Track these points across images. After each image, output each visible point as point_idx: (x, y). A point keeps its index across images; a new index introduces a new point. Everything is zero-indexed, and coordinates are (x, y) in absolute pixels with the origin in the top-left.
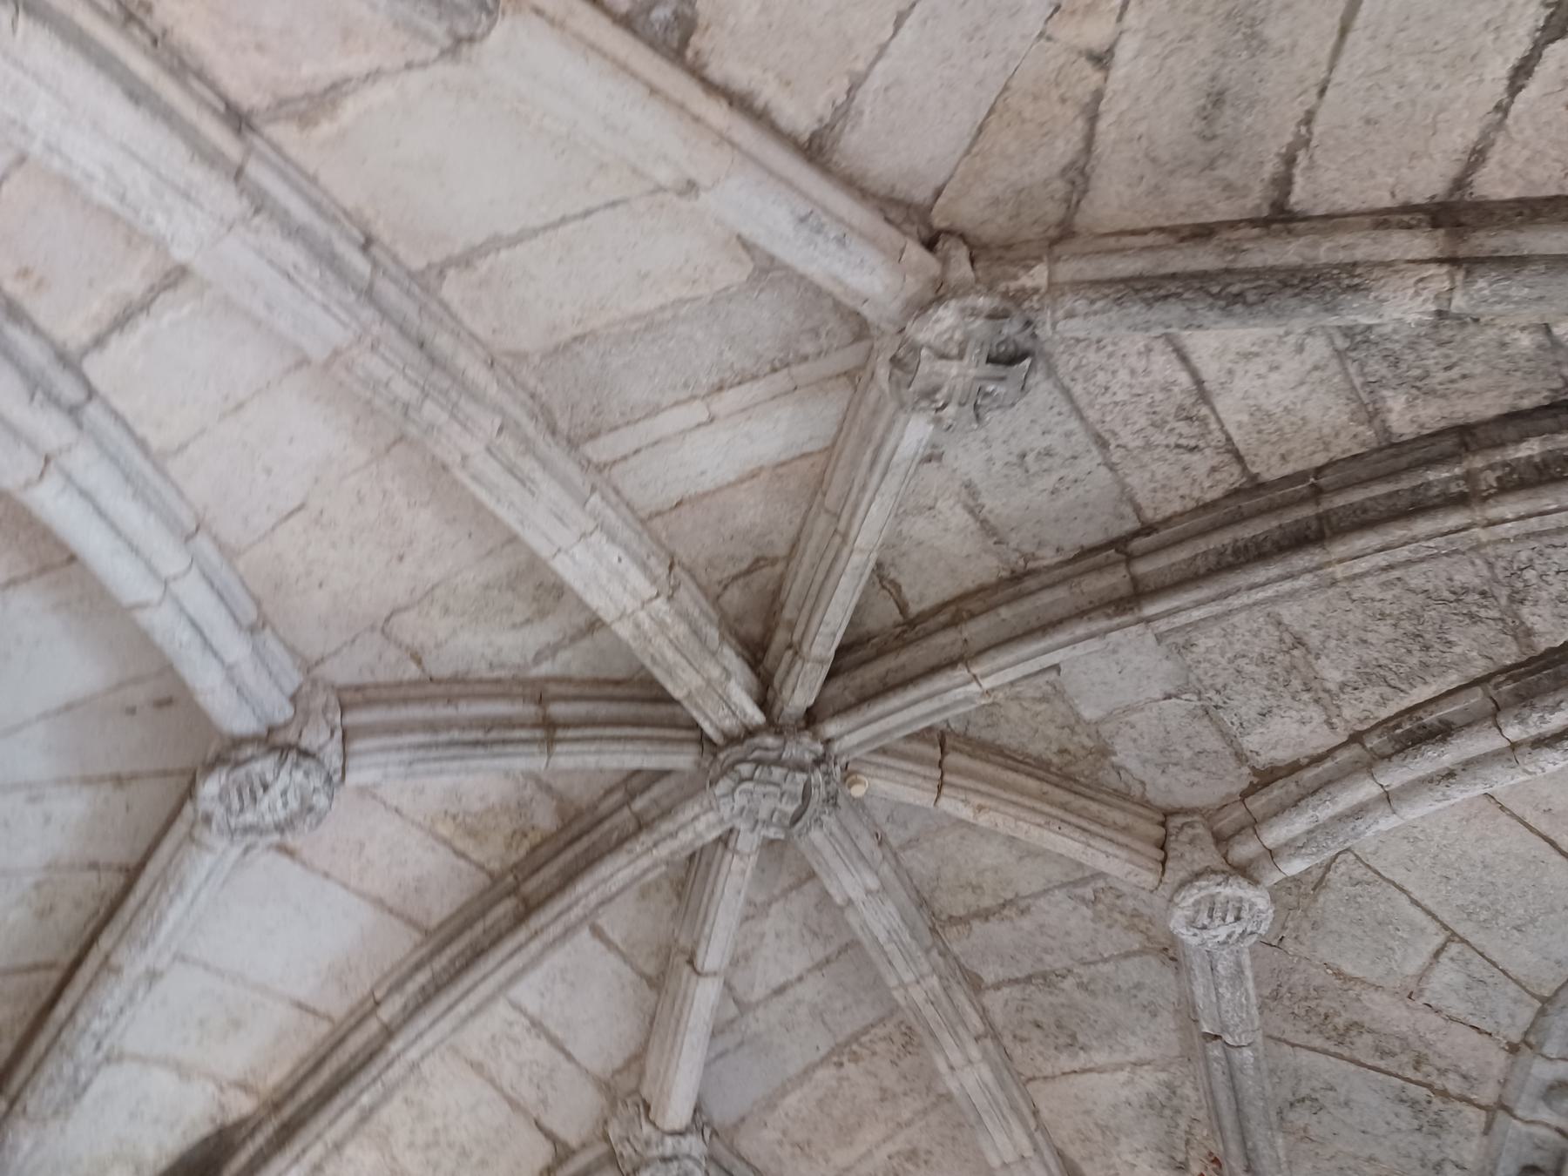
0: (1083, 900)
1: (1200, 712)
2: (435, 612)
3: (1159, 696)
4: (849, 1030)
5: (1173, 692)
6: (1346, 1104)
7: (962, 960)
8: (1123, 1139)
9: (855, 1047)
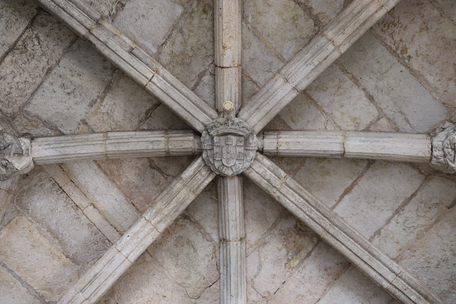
2: (189, 282)
4: (389, 57)
9: (399, 52)
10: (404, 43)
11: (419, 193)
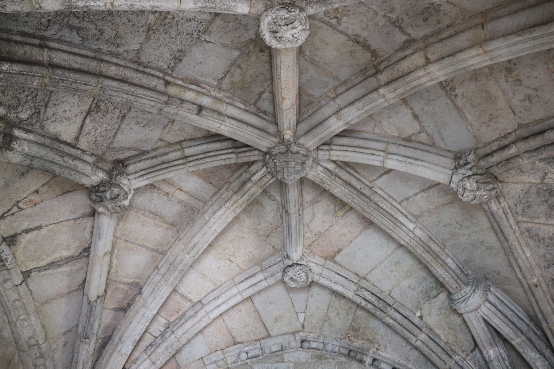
2: (260, 227)
9: (448, 88)
10: (454, 84)
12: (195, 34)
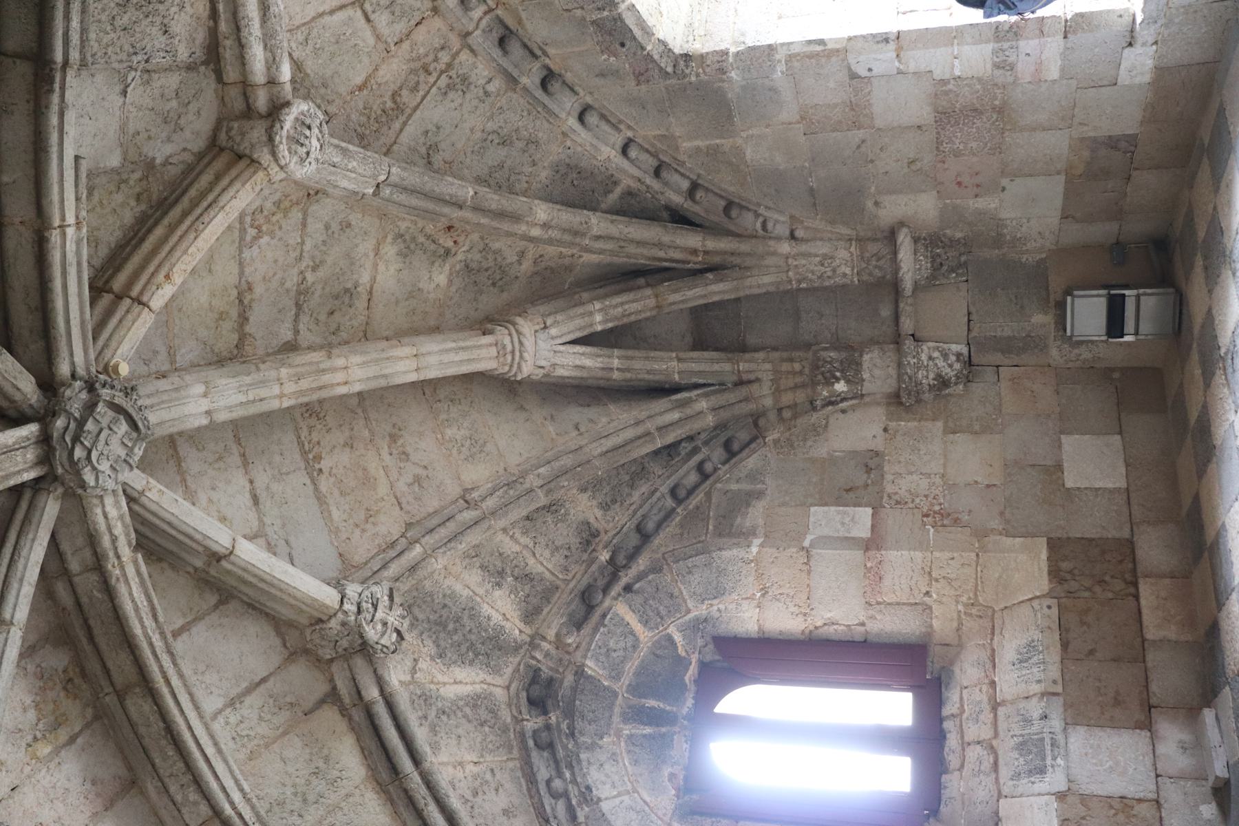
0: (256, 238)
1: (146, 76)
3: (122, 100)
4: (297, 456)
5: (122, 87)
6: (438, 128)
7: (270, 351)
8: (421, 285)
9: (311, 456)
11: (272, 679)
12: (139, 57)
